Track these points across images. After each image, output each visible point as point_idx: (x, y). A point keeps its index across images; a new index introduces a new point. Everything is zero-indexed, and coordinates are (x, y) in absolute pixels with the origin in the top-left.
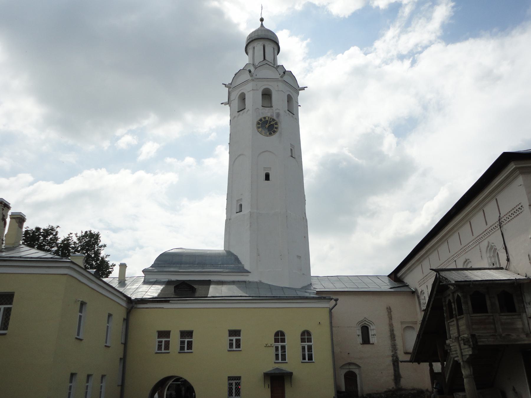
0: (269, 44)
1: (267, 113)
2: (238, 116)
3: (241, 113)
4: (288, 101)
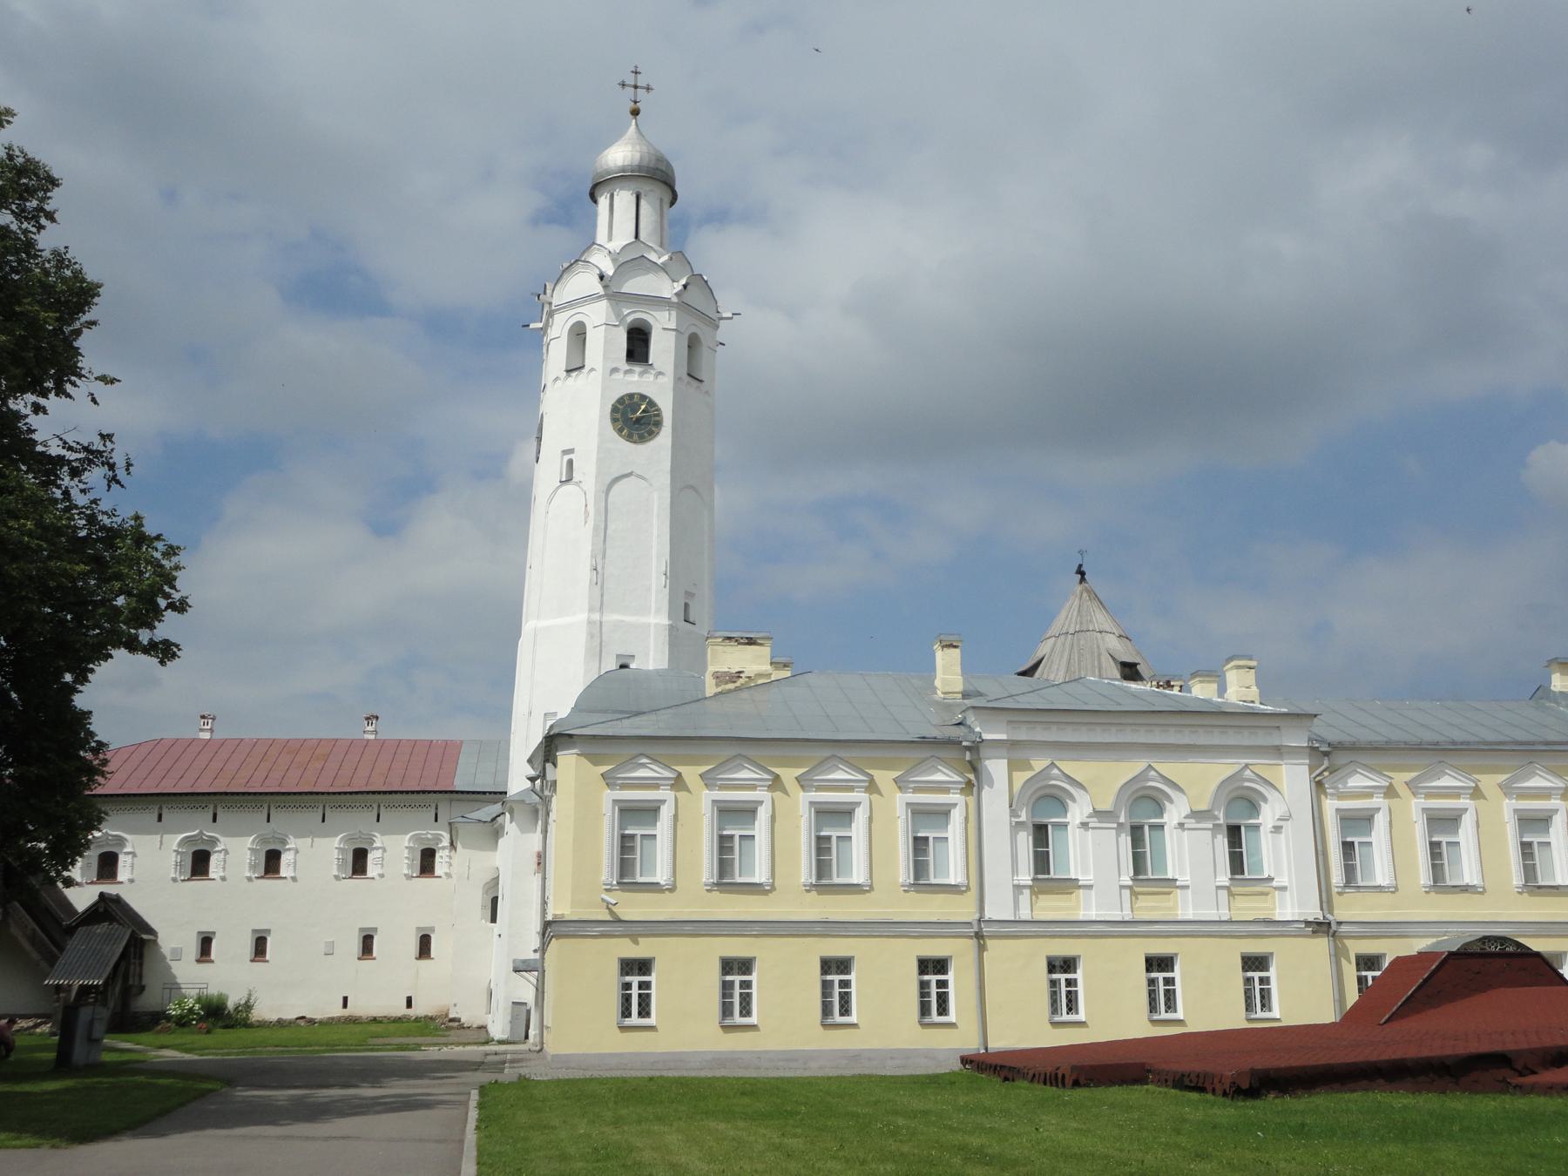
0: (651, 191)
1: (635, 381)
2: (566, 379)
3: (574, 374)
4: (689, 346)
